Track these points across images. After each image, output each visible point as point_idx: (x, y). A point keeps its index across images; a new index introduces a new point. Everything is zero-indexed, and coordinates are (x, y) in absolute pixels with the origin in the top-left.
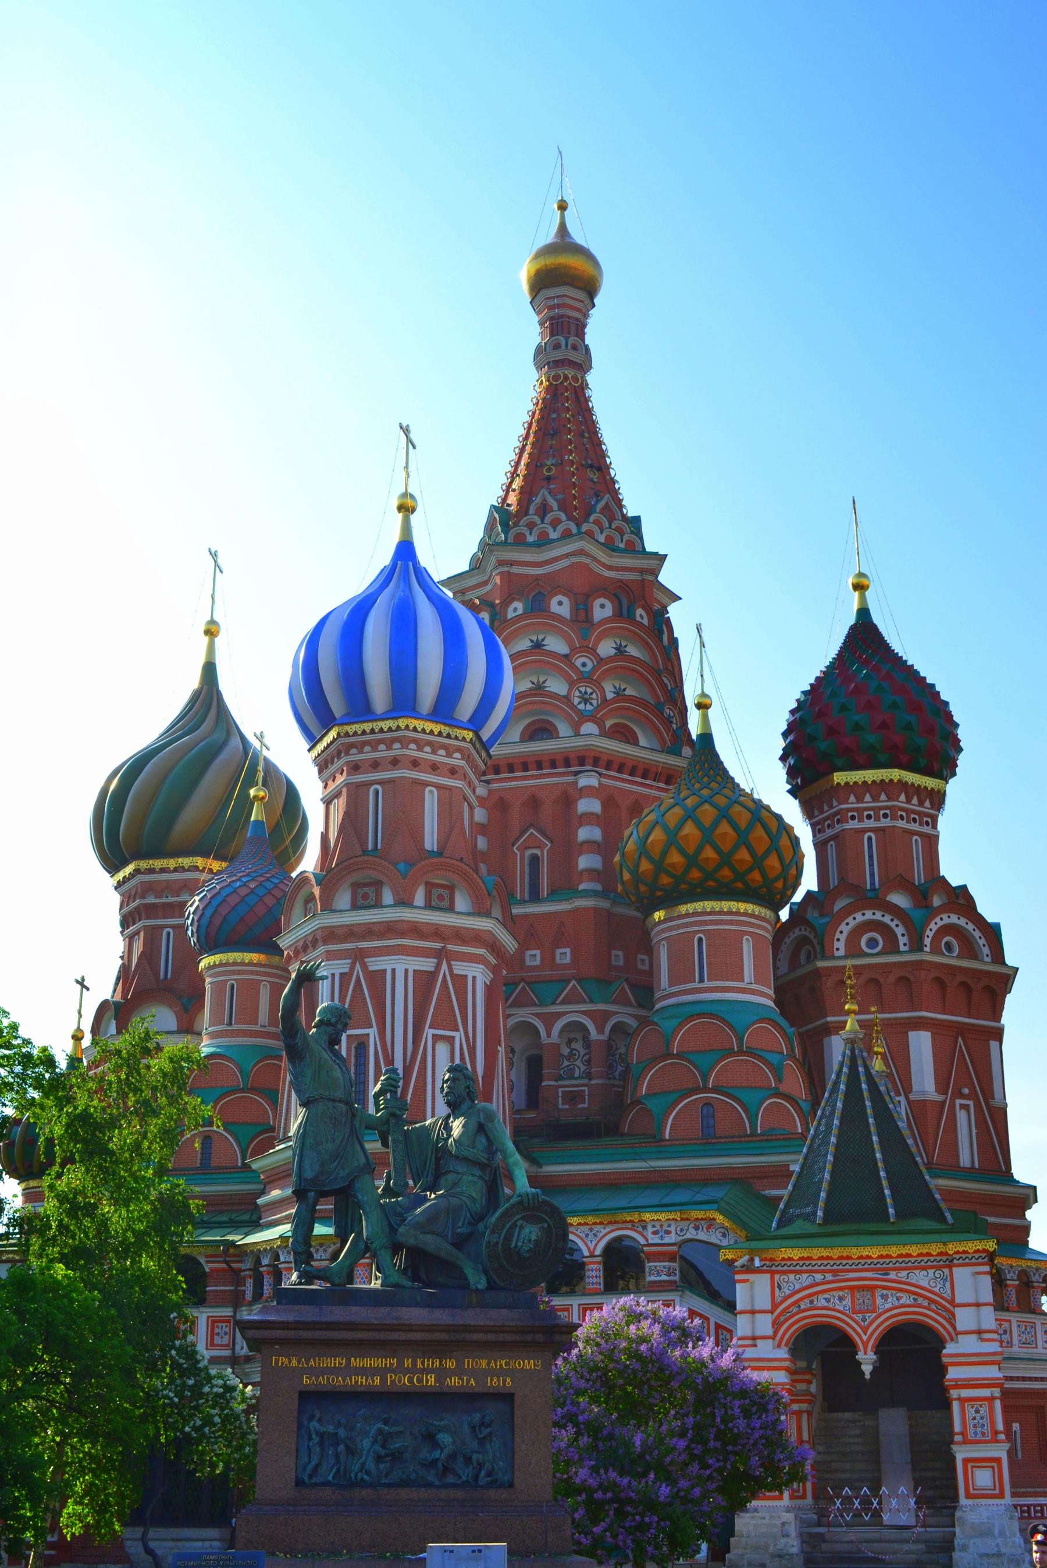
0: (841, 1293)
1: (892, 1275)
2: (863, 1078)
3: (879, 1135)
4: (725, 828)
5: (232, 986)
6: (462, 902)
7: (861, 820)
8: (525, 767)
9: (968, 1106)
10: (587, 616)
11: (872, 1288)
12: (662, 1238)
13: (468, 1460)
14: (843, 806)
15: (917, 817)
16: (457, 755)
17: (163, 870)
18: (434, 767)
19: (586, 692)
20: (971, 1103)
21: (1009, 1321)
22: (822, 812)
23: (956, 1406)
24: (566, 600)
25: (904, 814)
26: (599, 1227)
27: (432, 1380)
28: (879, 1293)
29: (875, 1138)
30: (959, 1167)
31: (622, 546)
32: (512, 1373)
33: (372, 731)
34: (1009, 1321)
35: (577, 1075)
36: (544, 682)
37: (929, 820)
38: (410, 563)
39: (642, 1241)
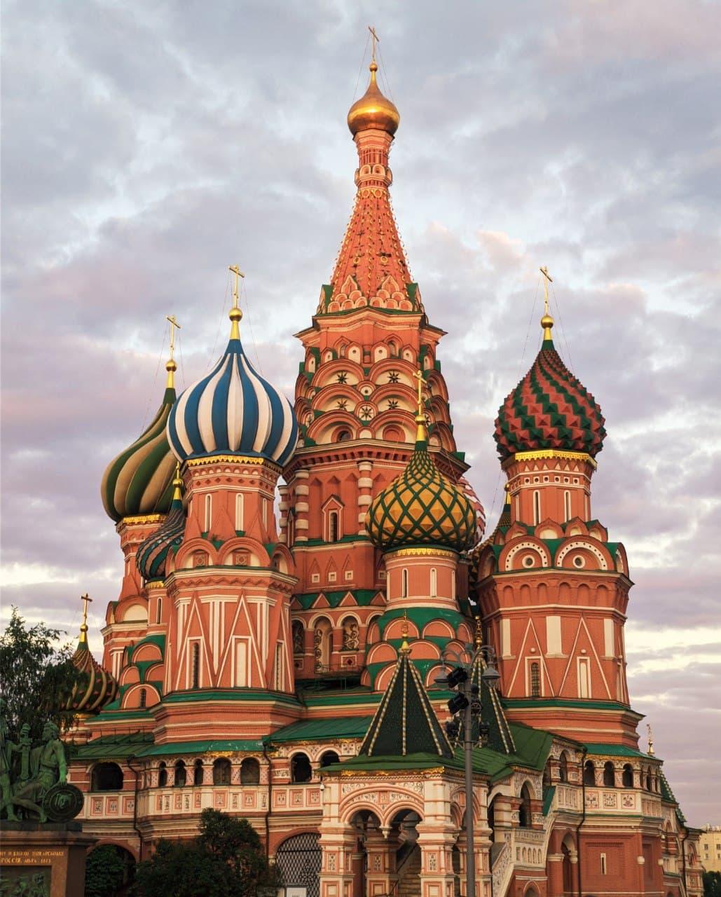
0: (373, 793)
1: (397, 785)
3: (407, 707)
4: (416, 505)
5: (160, 600)
6: (255, 562)
7: (532, 482)
8: (329, 459)
9: (586, 660)
10: (370, 359)
11: (386, 791)
12: (348, 752)
13: (32, 892)
15: (568, 478)
16: (256, 473)
17: (139, 523)
18: (241, 481)
19: (367, 410)
20: (588, 658)
23: (422, 853)
24: (358, 350)
25: (559, 477)
26: (318, 746)
27: (19, 860)
28: (391, 794)
29: (404, 709)
31: (398, 309)
32: (51, 857)
33: (205, 463)
35: (355, 647)
36: (345, 403)
38: (235, 354)
39: (339, 754)
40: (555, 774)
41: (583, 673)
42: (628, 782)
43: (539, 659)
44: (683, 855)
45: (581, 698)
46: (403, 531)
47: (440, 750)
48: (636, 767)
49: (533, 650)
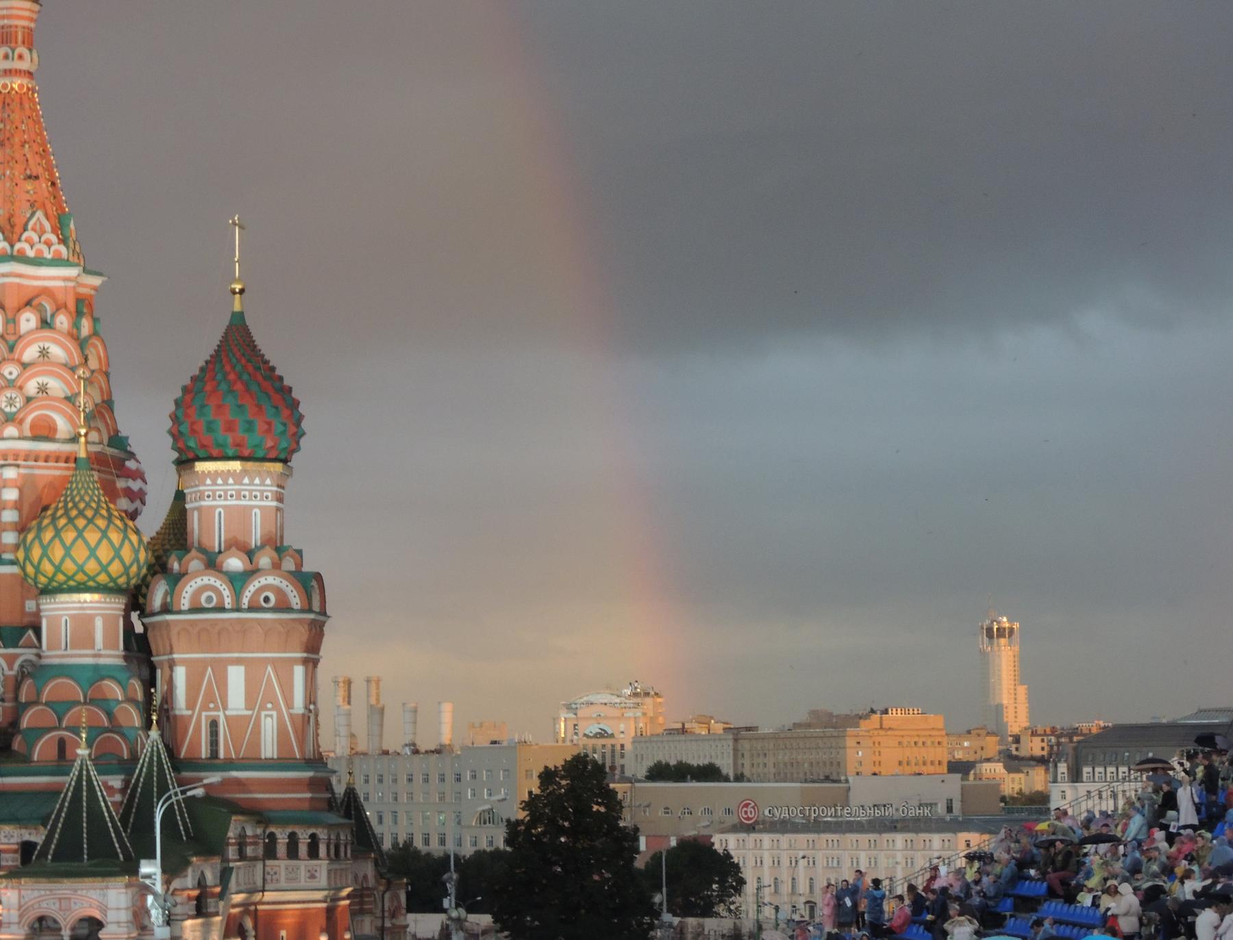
0: (54, 901)
1: (79, 892)
2: (84, 778)
7: (214, 499)
9: (271, 716)
11: (70, 899)
12: (9, 839)
14: (201, 488)
19: (11, 398)
20: (274, 713)
21: (279, 866)
22: (192, 487)
28: (72, 901)
30: (261, 759)
31: (49, 256)
34: (279, 866)
37: (269, 494)
40: (232, 852)
41: (269, 727)
42: (313, 853)
43: (219, 716)
44: (383, 911)
45: (266, 759)
46: (64, 574)
47: (121, 856)
48: (322, 834)
49: (212, 705)
